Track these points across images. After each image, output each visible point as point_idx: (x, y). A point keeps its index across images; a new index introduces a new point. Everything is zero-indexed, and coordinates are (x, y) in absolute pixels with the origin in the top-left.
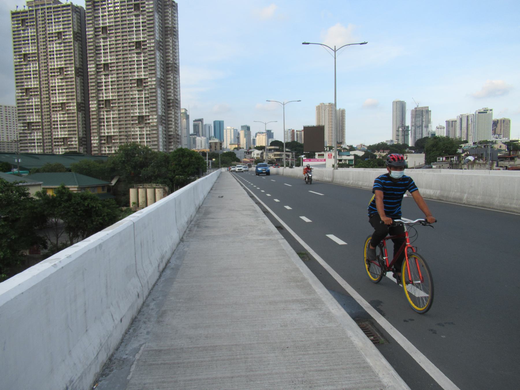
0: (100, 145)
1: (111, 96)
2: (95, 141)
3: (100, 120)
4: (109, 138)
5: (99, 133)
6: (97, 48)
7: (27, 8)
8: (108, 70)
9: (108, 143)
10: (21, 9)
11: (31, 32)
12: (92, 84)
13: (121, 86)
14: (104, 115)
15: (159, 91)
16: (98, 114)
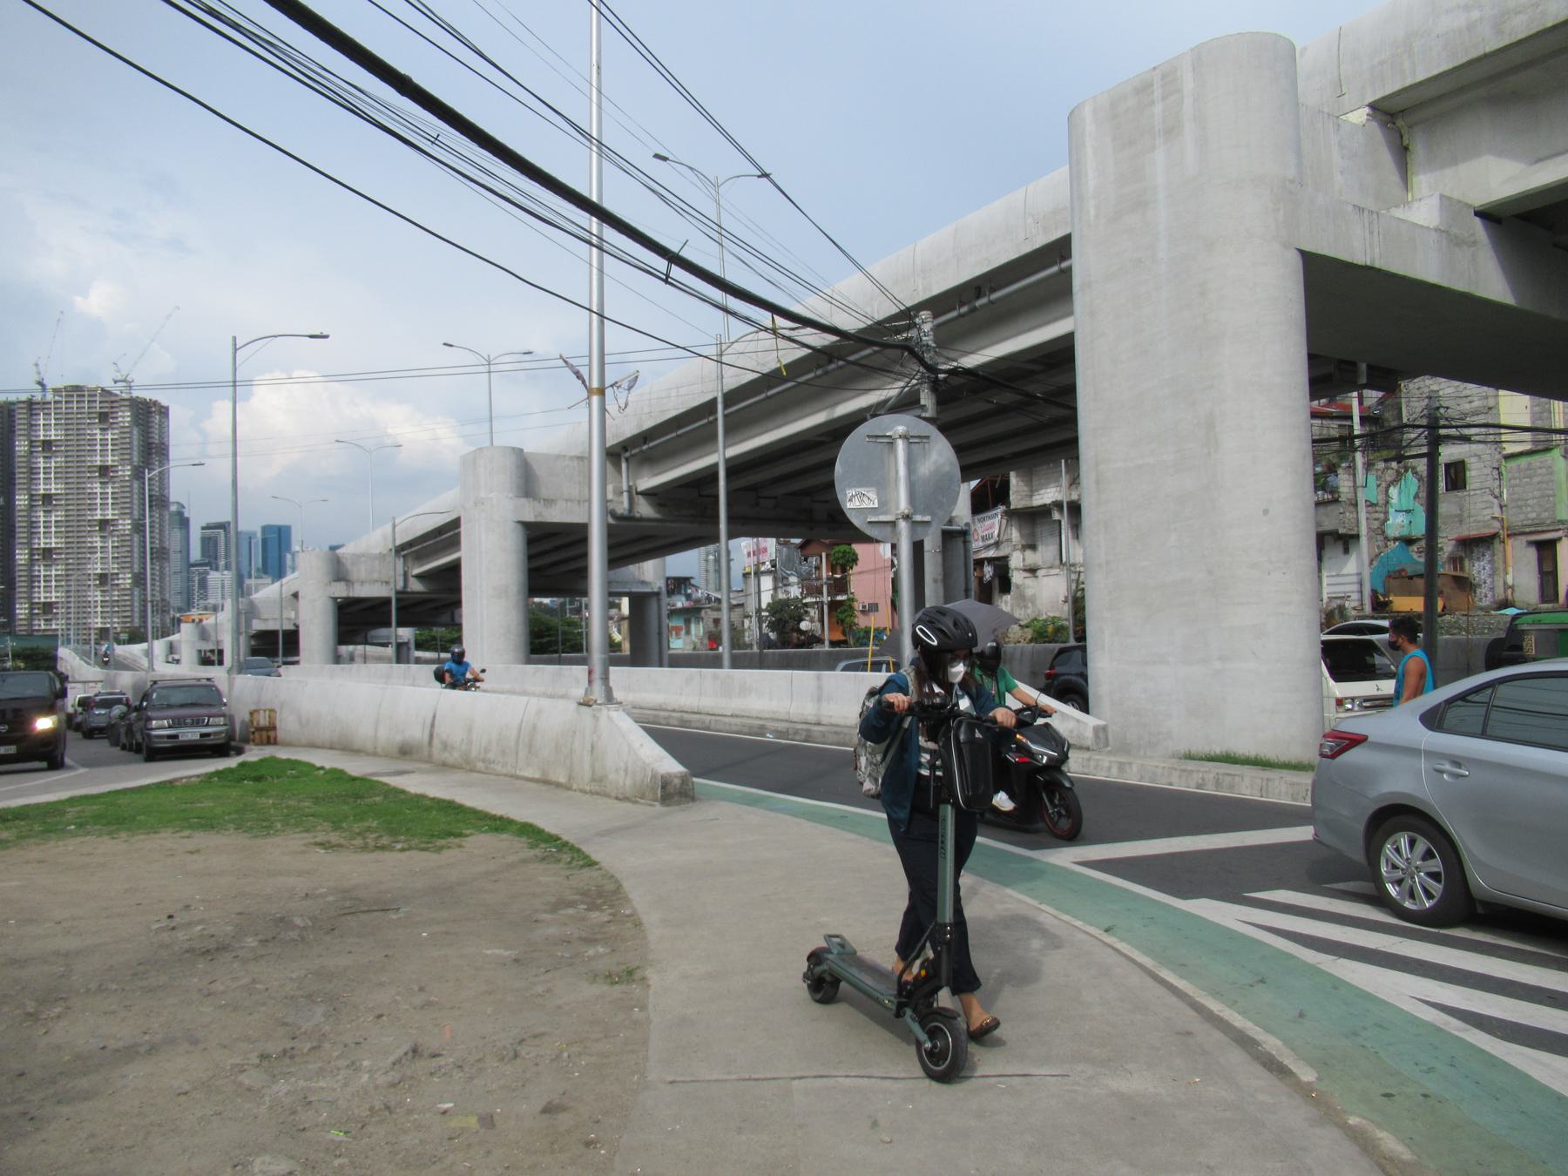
0: (32, 616)
1: (54, 542)
2: (21, 610)
3: (32, 579)
4: (48, 607)
5: (30, 598)
8: (50, 503)
9: (45, 613)
13: (74, 529)
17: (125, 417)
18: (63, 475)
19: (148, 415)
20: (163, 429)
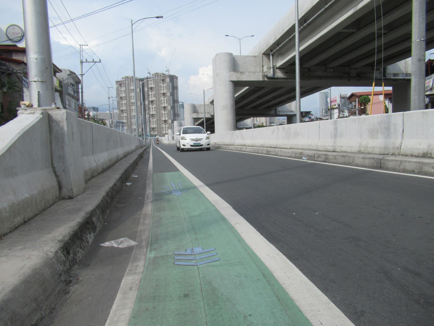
1: (154, 113)
4: (153, 129)
6: (148, 95)
7: (122, 80)
10: (119, 80)
11: (123, 89)
12: (147, 108)
13: (157, 109)
14: (152, 120)
15: (172, 111)
16: (149, 120)
17: (168, 80)
18: (155, 96)
19: (173, 79)
20: (177, 82)
